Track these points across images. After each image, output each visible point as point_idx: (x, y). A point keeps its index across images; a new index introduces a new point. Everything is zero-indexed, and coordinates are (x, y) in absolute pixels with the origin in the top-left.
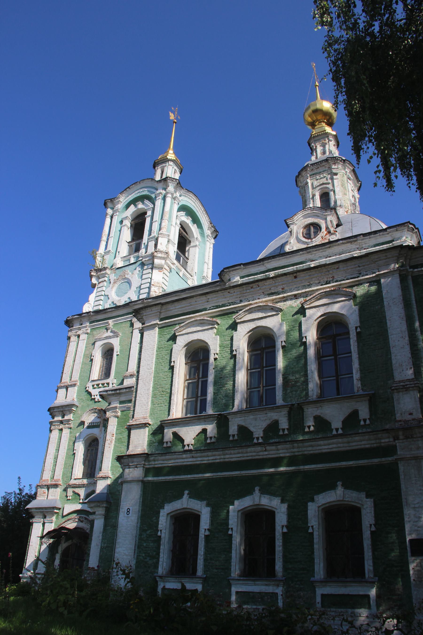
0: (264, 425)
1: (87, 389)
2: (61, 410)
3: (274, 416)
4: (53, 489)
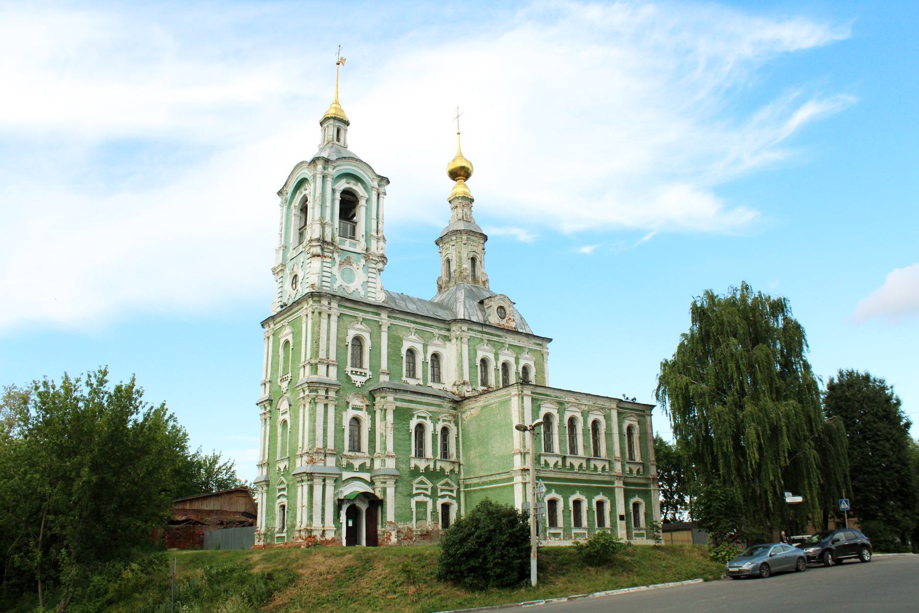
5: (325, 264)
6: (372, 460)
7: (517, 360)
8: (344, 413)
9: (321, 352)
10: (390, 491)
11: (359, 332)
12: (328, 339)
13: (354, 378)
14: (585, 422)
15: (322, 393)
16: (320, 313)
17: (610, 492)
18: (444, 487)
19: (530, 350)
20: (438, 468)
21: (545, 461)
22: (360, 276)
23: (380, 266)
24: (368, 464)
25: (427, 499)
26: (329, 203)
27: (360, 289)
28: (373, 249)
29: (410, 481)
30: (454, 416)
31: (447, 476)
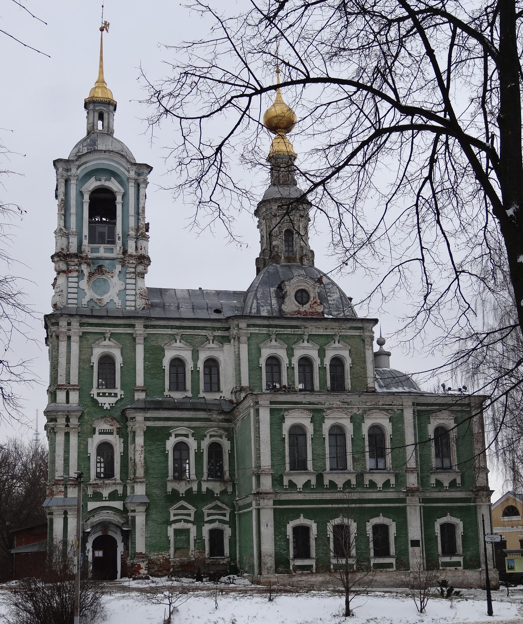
0: (344, 481)
1: (92, 396)
2: (67, 413)
3: (348, 477)
4: (71, 489)
5: (70, 279)
6: (125, 487)
7: (322, 354)
8: (90, 440)
9: (59, 378)
10: (140, 520)
11: (106, 350)
12: (68, 362)
13: (101, 400)
14: (357, 428)
15: (61, 421)
16: (57, 337)
17: (400, 515)
18: (212, 511)
19: (343, 338)
20: (204, 489)
21: (290, 482)
22: (115, 284)
23: (140, 268)
24: (120, 492)
25: (190, 525)
26: (73, 210)
27: (116, 300)
28: (131, 250)
29: (168, 507)
30: (225, 429)
31: (218, 498)
